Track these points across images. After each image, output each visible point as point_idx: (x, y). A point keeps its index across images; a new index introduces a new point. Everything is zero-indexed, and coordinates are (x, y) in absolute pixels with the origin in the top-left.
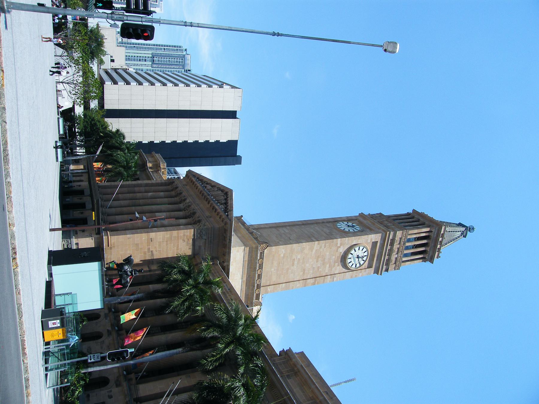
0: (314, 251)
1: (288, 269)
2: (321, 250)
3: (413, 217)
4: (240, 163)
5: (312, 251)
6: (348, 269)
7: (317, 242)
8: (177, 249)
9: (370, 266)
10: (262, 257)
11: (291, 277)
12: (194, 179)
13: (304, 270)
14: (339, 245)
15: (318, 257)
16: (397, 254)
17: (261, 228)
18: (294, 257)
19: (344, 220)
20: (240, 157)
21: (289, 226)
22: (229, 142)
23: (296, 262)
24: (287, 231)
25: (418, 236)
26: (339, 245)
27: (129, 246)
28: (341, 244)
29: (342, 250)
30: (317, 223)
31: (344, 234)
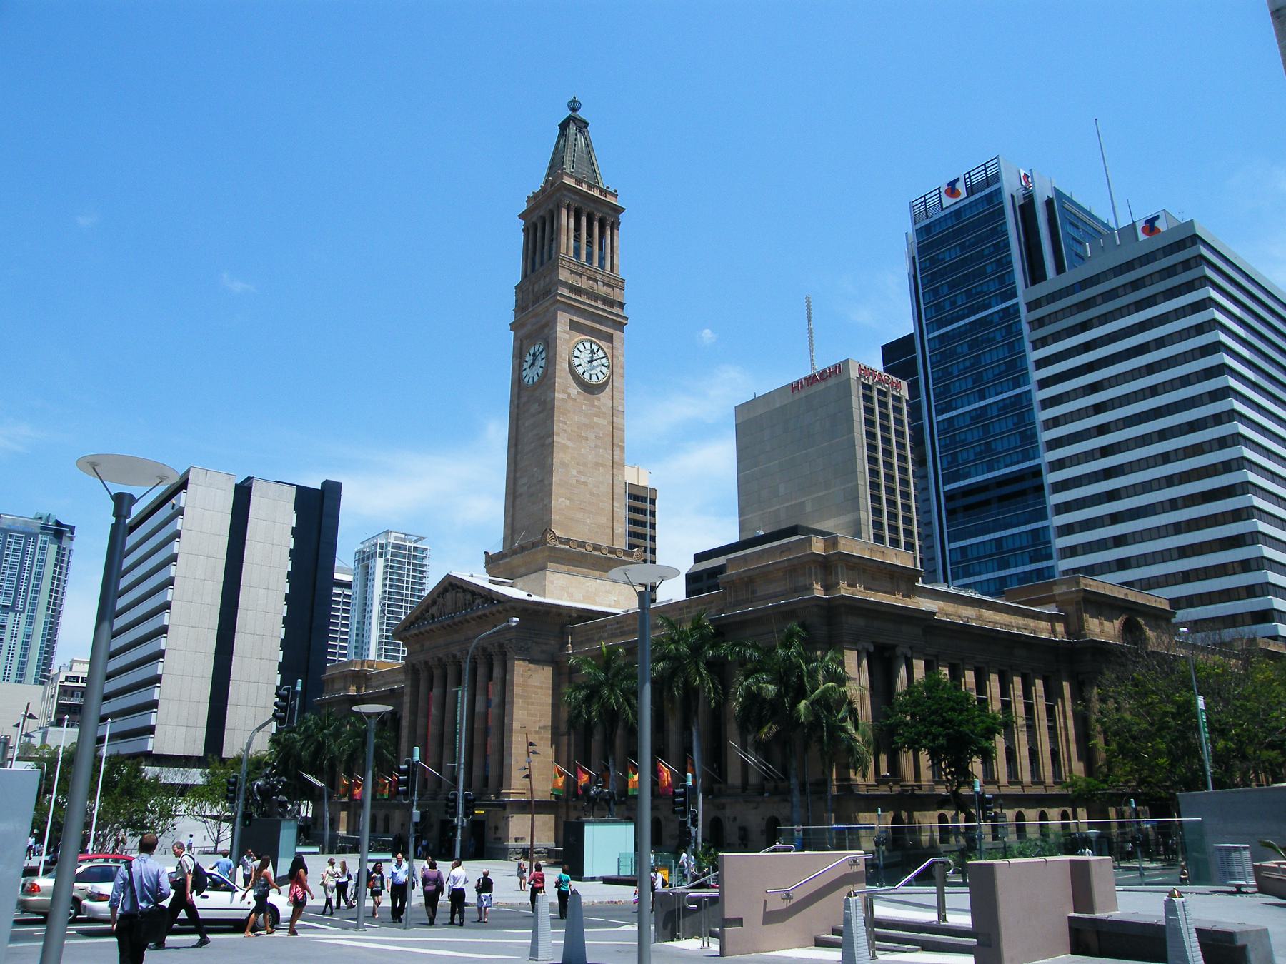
0: (569, 443)
1: (592, 494)
2: (569, 429)
3: (535, 225)
4: (339, 485)
5: (568, 447)
6: (605, 384)
7: (555, 438)
8: (541, 688)
9: (610, 338)
10: (567, 542)
11: (606, 489)
12: (414, 631)
13: (597, 464)
14: (565, 397)
15: (580, 436)
16: (596, 281)
17: (513, 524)
18: (573, 481)
19: (520, 365)
20: (326, 484)
21: (515, 471)
22: (298, 508)
23: (583, 479)
24: (524, 480)
25: (572, 234)
26: (565, 397)
27: (534, 765)
28: (565, 389)
29: (575, 390)
30: (518, 420)
31: (547, 379)
